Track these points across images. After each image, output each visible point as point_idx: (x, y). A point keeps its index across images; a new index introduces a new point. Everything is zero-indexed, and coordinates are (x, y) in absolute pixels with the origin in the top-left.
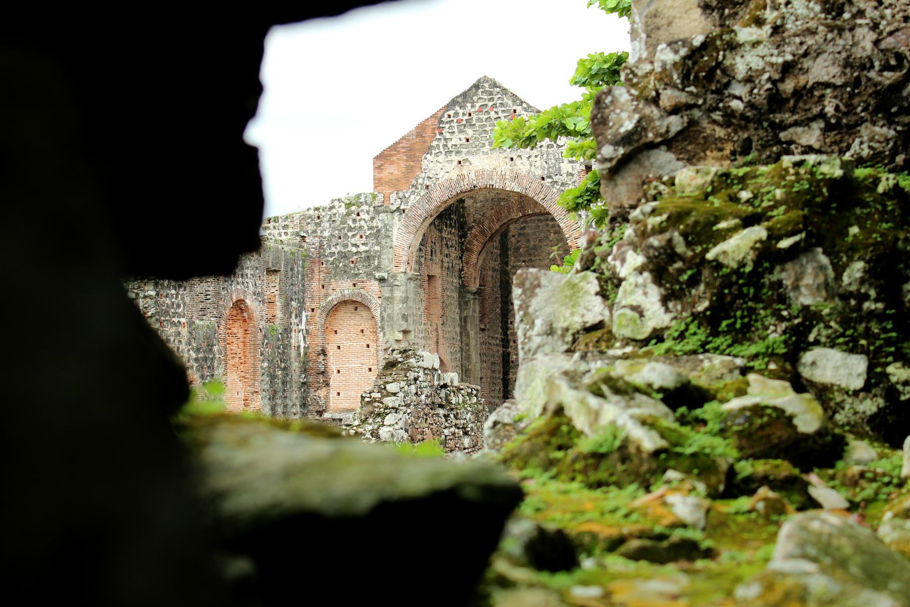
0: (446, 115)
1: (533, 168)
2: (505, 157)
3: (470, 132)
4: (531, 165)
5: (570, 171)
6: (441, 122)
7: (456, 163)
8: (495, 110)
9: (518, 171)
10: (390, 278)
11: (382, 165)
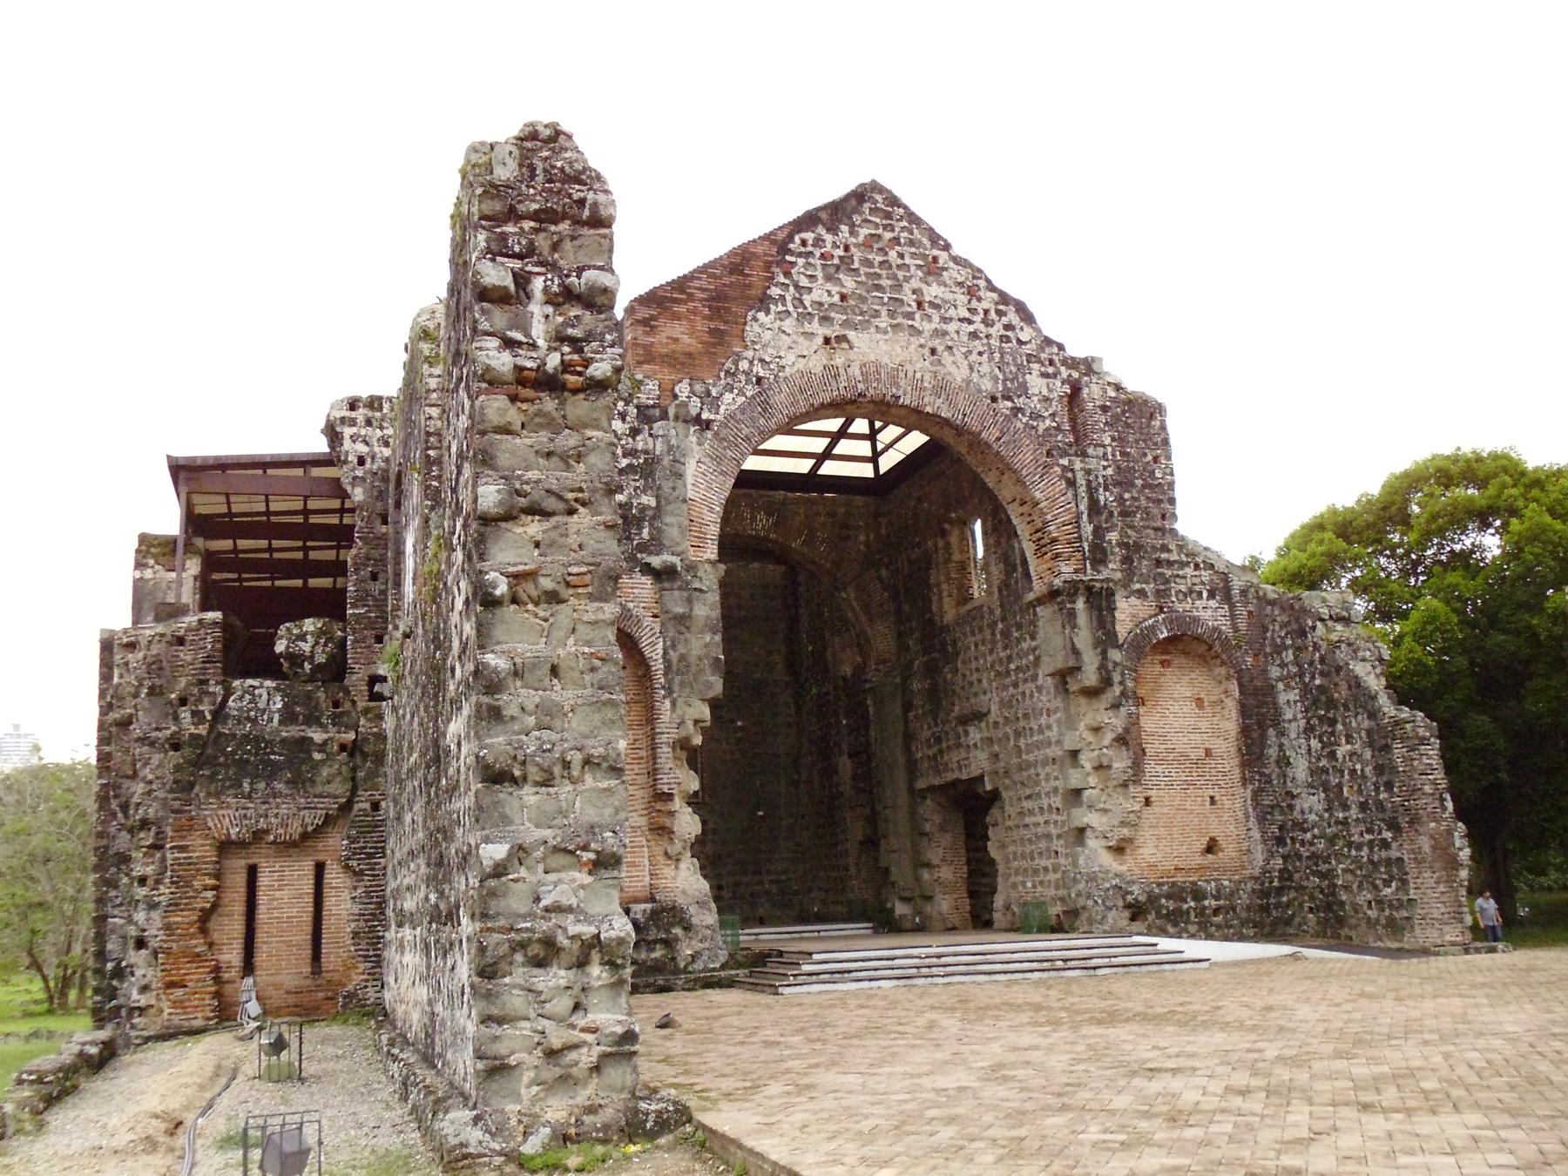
0: (797, 239)
1: (975, 375)
2: (921, 346)
3: (849, 283)
4: (971, 368)
5: (1045, 392)
6: (784, 249)
7: (820, 340)
8: (898, 248)
9: (948, 377)
10: (684, 573)
11: (652, 318)
